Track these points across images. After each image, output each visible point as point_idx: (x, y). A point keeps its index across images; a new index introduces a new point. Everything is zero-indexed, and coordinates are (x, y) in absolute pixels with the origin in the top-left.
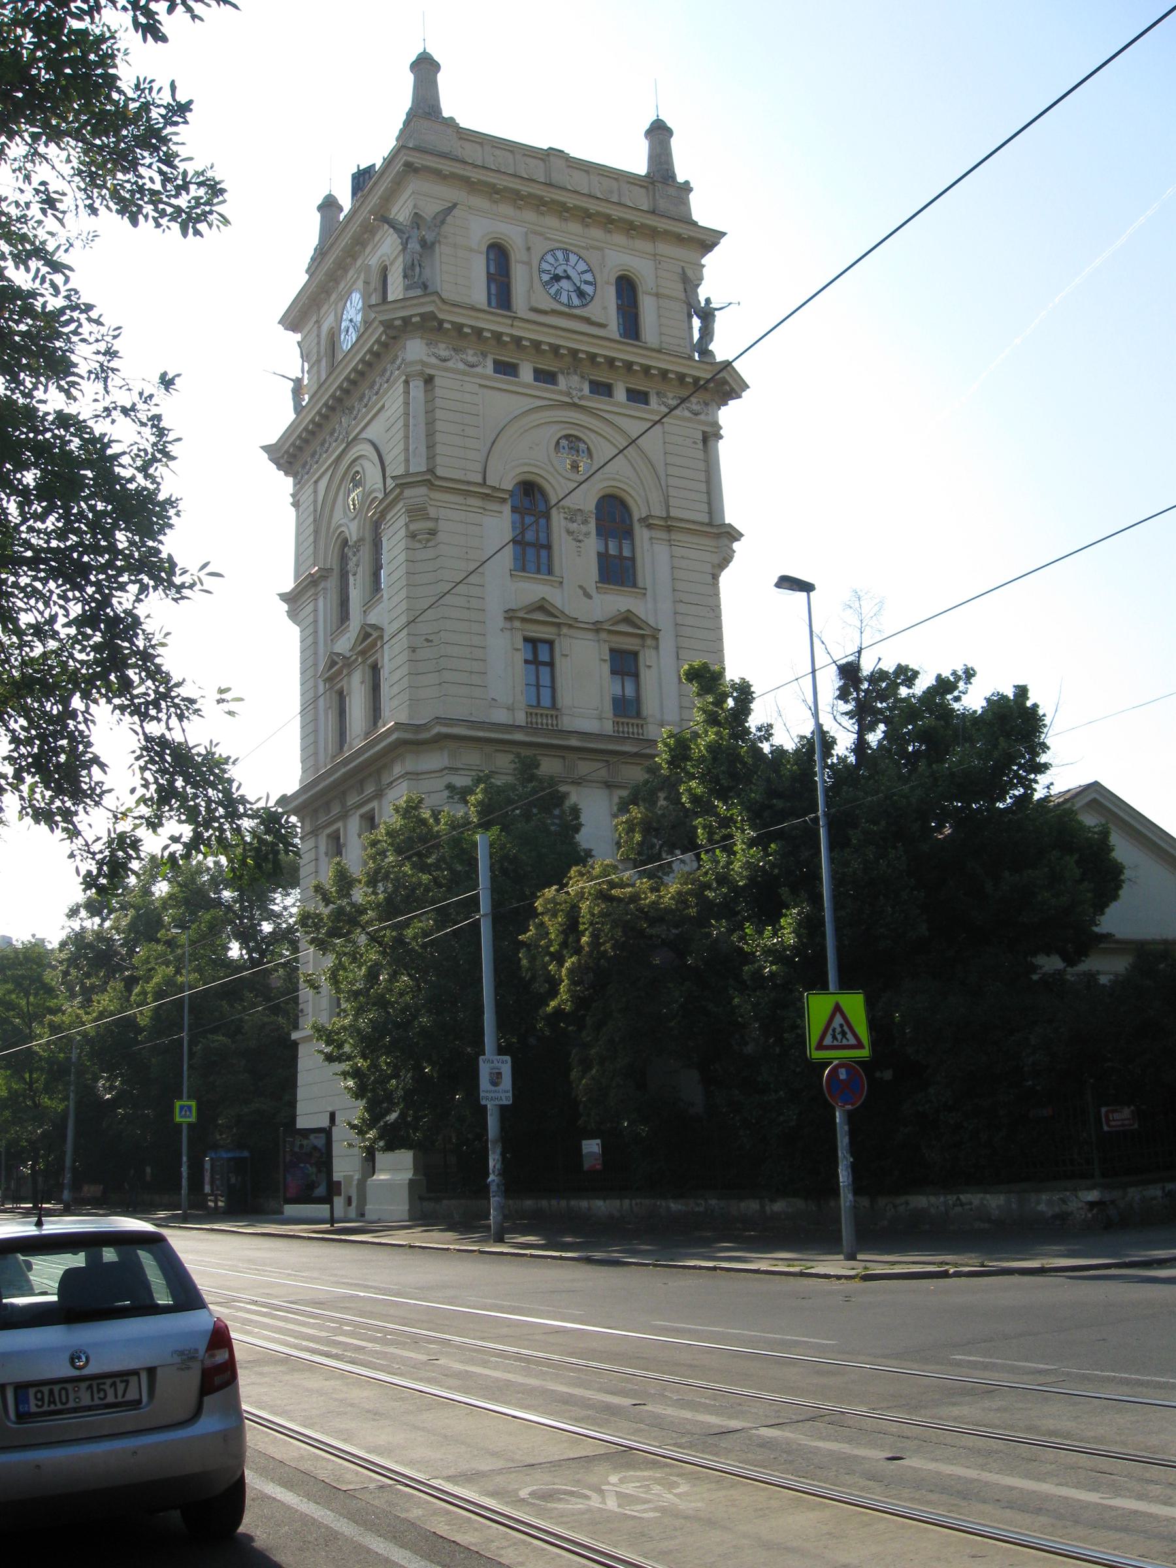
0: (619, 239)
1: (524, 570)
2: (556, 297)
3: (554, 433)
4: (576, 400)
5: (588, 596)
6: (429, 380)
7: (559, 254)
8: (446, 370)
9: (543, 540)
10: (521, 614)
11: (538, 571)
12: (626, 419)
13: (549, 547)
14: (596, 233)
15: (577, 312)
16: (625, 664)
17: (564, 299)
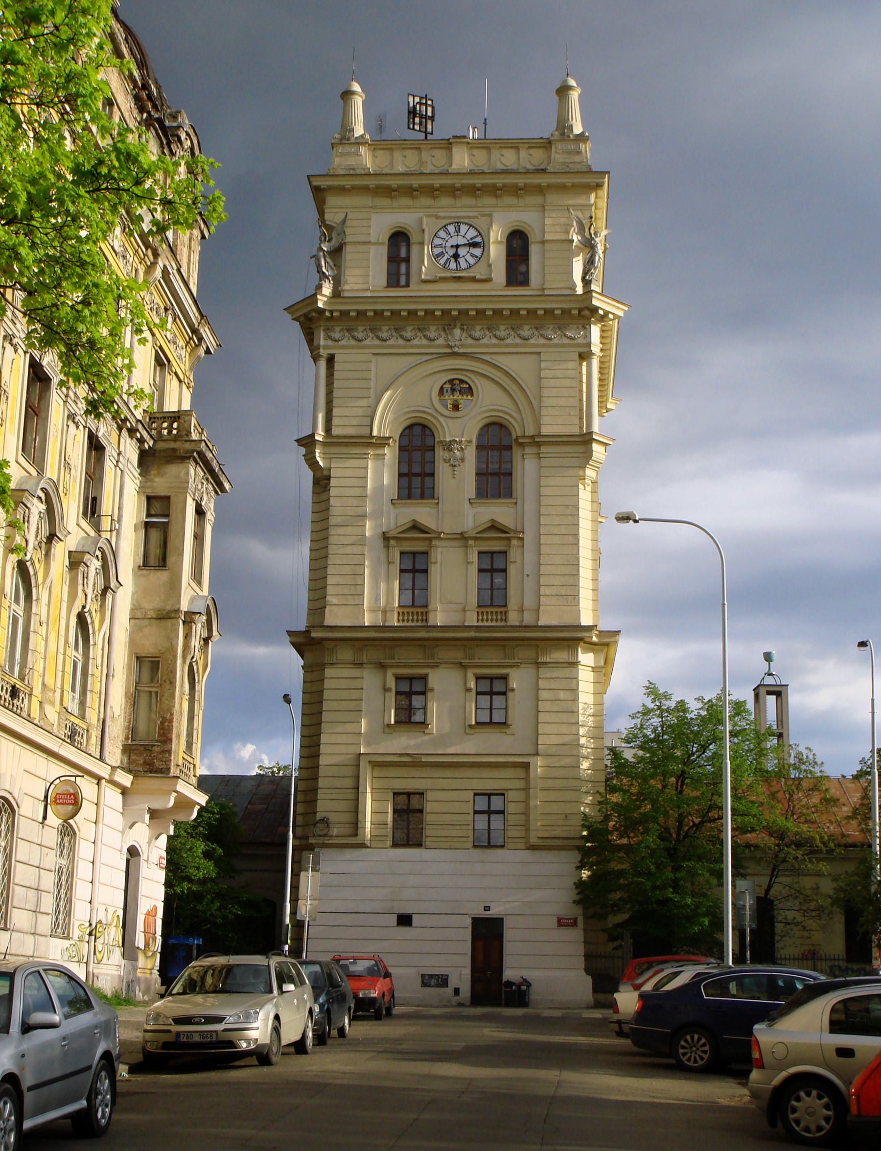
0: (509, 200)
1: (410, 497)
4: (456, 349)
7: (451, 229)
8: (343, 347)
9: (428, 470)
11: (422, 497)
12: (504, 357)
13: (433, 475)
14: (488, 200)
16: (493, 567)
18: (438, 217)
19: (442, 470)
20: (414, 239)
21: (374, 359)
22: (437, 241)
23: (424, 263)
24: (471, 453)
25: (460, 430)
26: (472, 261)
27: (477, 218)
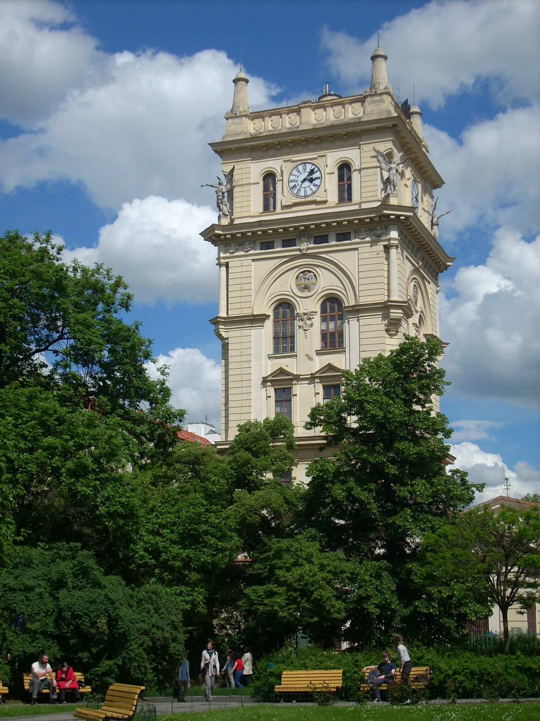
2: (297, 196)
3: (294, 273)
4: (305, 252)
5: (311, 359)
6: (227, 265)
10: (270, 378)
15: (310, 199)
17: (302, 193)
18: (293, 162)
19: (299, 334)
20: (278, 177)
21: (253, 263)
22: (292, 178)
23: (284, 196)
24: (317, 319)
25: (309, 305)
26: (314, 189)
27: (316, 158)
